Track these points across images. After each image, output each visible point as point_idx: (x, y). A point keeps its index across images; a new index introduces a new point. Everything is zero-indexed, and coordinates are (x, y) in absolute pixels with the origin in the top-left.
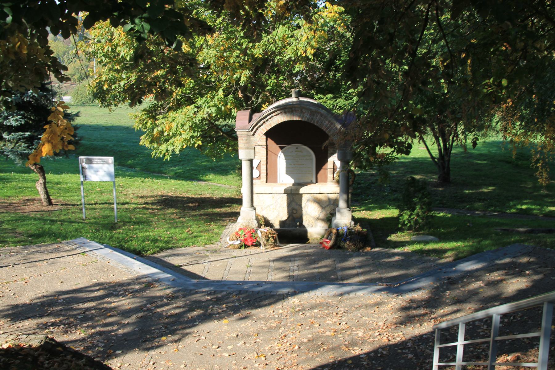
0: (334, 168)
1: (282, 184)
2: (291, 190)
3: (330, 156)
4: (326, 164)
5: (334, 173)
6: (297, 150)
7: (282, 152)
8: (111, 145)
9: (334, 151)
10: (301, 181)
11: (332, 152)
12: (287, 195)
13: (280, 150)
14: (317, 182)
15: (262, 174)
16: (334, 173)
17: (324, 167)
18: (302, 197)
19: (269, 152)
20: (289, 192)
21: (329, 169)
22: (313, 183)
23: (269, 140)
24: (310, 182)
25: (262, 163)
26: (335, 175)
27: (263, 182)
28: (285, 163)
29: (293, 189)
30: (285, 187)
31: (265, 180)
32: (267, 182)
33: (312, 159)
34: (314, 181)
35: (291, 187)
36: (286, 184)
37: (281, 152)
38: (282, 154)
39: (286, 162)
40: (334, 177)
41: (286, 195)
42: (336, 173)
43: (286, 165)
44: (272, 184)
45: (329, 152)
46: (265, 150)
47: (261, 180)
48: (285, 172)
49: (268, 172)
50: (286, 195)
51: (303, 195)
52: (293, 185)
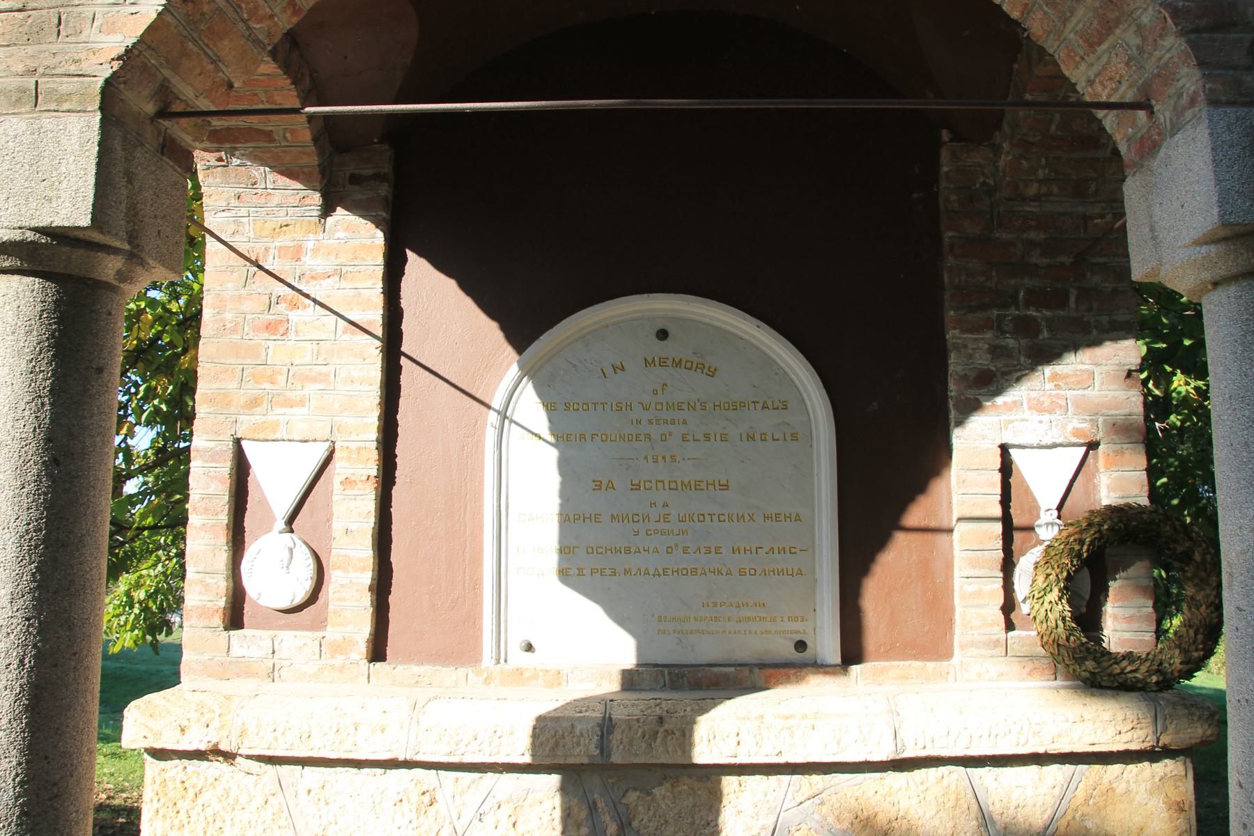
0: (1006, 519)
1: (519, 675)
2: (607, 726)
3: (973, 406)
4: (937, 487)
5: (1008, 566)
6: (660, 348)
7: (528, 371)
8: (167, 672)
9: (996, 351)
10: (707, 650)
11: (982, 360)
12: (563, 789)
13: (509, 351)
14: (852, 654)
15: (335, 578)
16: (1008, 566)
17: (915, 516)
18: (714, 800)
19: (409, 375)
20: (581, 754)
21: (961, 530)
22: (818, 667)
23: (417, 268)
24: (786, 650)
25: (339, 468)
26: (1021, 587)
27: (337, 649)
28: (554, 480)
29: (618, 714)
30: (548, 702)
31: (365, 628)
32: (378, 652)
33: (800, 436)
34: (829, 645)
35: (606, 701)
36: (557, 678)
37: (514, 370)
38: (528, 392)
39: (564, 465)
40: (1009, 607)
41: (554, 780)
42: (1025, 565)
43: (563, 494)
44: (425, 669)
45: (955, 364)
46: (373, 351)
47: (332, 633)
48: (552, 560)
49: (395, 558)
50: (554, 780)
51: (729, 783)
52: (630, 680)
